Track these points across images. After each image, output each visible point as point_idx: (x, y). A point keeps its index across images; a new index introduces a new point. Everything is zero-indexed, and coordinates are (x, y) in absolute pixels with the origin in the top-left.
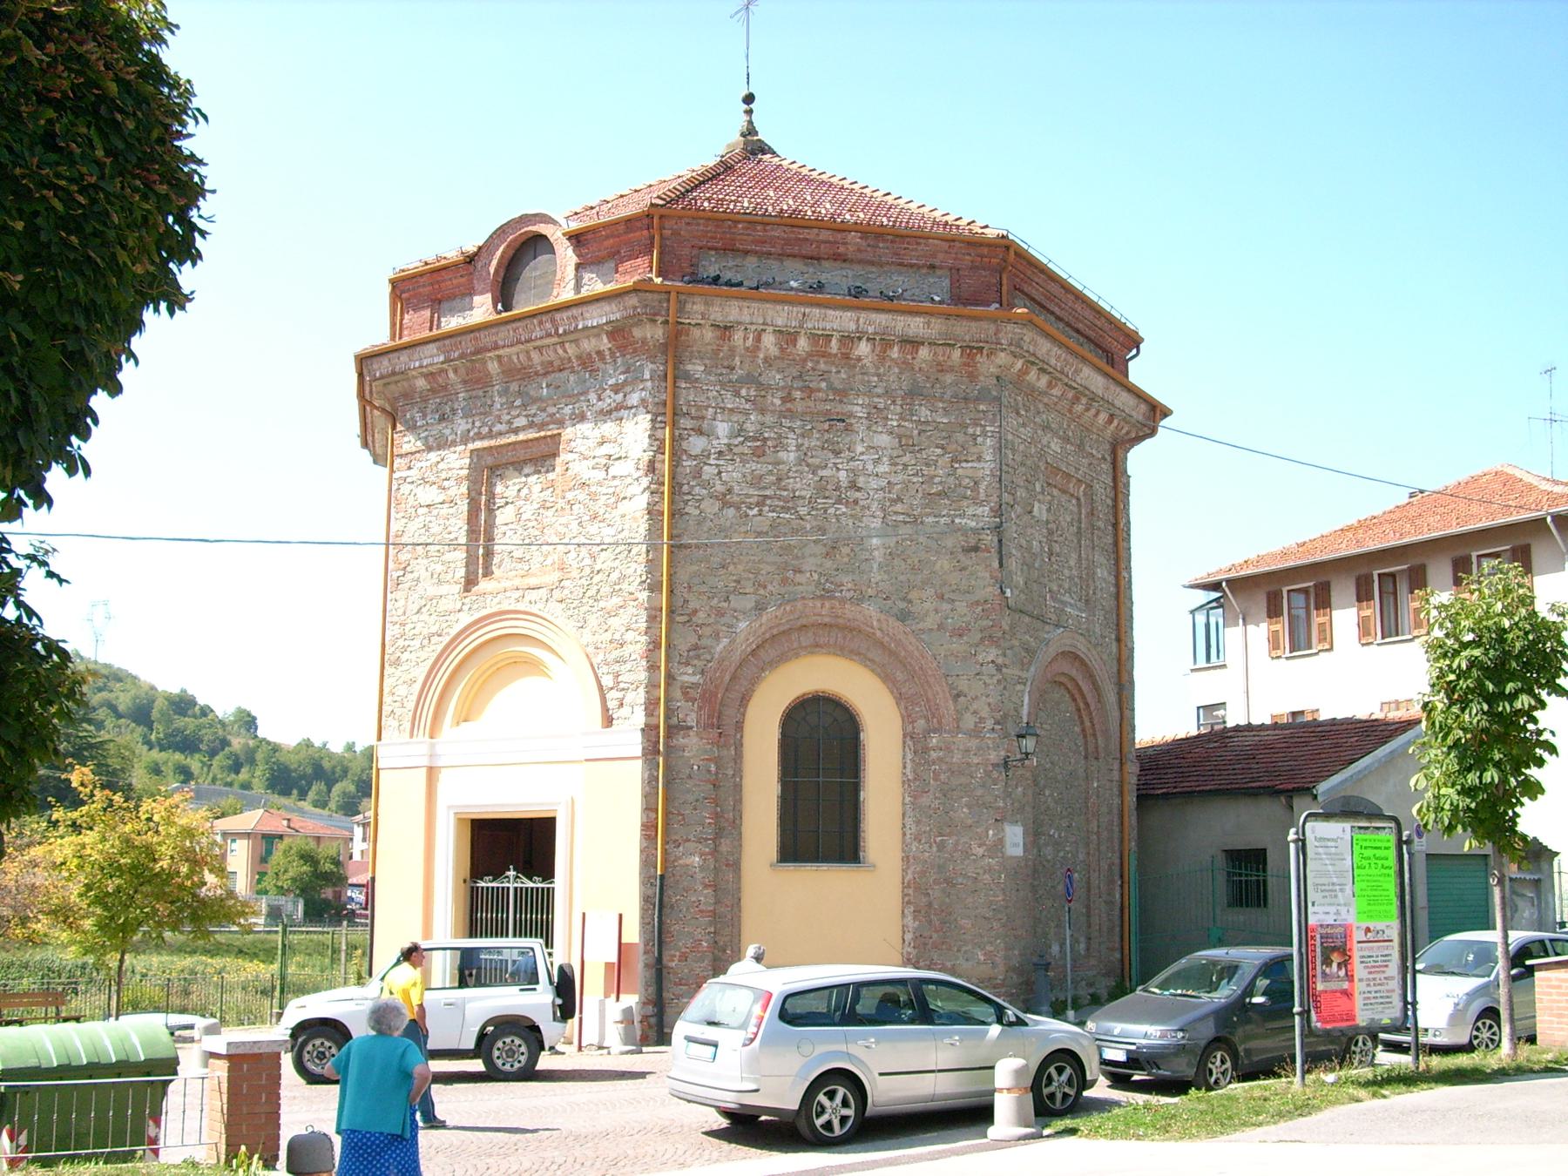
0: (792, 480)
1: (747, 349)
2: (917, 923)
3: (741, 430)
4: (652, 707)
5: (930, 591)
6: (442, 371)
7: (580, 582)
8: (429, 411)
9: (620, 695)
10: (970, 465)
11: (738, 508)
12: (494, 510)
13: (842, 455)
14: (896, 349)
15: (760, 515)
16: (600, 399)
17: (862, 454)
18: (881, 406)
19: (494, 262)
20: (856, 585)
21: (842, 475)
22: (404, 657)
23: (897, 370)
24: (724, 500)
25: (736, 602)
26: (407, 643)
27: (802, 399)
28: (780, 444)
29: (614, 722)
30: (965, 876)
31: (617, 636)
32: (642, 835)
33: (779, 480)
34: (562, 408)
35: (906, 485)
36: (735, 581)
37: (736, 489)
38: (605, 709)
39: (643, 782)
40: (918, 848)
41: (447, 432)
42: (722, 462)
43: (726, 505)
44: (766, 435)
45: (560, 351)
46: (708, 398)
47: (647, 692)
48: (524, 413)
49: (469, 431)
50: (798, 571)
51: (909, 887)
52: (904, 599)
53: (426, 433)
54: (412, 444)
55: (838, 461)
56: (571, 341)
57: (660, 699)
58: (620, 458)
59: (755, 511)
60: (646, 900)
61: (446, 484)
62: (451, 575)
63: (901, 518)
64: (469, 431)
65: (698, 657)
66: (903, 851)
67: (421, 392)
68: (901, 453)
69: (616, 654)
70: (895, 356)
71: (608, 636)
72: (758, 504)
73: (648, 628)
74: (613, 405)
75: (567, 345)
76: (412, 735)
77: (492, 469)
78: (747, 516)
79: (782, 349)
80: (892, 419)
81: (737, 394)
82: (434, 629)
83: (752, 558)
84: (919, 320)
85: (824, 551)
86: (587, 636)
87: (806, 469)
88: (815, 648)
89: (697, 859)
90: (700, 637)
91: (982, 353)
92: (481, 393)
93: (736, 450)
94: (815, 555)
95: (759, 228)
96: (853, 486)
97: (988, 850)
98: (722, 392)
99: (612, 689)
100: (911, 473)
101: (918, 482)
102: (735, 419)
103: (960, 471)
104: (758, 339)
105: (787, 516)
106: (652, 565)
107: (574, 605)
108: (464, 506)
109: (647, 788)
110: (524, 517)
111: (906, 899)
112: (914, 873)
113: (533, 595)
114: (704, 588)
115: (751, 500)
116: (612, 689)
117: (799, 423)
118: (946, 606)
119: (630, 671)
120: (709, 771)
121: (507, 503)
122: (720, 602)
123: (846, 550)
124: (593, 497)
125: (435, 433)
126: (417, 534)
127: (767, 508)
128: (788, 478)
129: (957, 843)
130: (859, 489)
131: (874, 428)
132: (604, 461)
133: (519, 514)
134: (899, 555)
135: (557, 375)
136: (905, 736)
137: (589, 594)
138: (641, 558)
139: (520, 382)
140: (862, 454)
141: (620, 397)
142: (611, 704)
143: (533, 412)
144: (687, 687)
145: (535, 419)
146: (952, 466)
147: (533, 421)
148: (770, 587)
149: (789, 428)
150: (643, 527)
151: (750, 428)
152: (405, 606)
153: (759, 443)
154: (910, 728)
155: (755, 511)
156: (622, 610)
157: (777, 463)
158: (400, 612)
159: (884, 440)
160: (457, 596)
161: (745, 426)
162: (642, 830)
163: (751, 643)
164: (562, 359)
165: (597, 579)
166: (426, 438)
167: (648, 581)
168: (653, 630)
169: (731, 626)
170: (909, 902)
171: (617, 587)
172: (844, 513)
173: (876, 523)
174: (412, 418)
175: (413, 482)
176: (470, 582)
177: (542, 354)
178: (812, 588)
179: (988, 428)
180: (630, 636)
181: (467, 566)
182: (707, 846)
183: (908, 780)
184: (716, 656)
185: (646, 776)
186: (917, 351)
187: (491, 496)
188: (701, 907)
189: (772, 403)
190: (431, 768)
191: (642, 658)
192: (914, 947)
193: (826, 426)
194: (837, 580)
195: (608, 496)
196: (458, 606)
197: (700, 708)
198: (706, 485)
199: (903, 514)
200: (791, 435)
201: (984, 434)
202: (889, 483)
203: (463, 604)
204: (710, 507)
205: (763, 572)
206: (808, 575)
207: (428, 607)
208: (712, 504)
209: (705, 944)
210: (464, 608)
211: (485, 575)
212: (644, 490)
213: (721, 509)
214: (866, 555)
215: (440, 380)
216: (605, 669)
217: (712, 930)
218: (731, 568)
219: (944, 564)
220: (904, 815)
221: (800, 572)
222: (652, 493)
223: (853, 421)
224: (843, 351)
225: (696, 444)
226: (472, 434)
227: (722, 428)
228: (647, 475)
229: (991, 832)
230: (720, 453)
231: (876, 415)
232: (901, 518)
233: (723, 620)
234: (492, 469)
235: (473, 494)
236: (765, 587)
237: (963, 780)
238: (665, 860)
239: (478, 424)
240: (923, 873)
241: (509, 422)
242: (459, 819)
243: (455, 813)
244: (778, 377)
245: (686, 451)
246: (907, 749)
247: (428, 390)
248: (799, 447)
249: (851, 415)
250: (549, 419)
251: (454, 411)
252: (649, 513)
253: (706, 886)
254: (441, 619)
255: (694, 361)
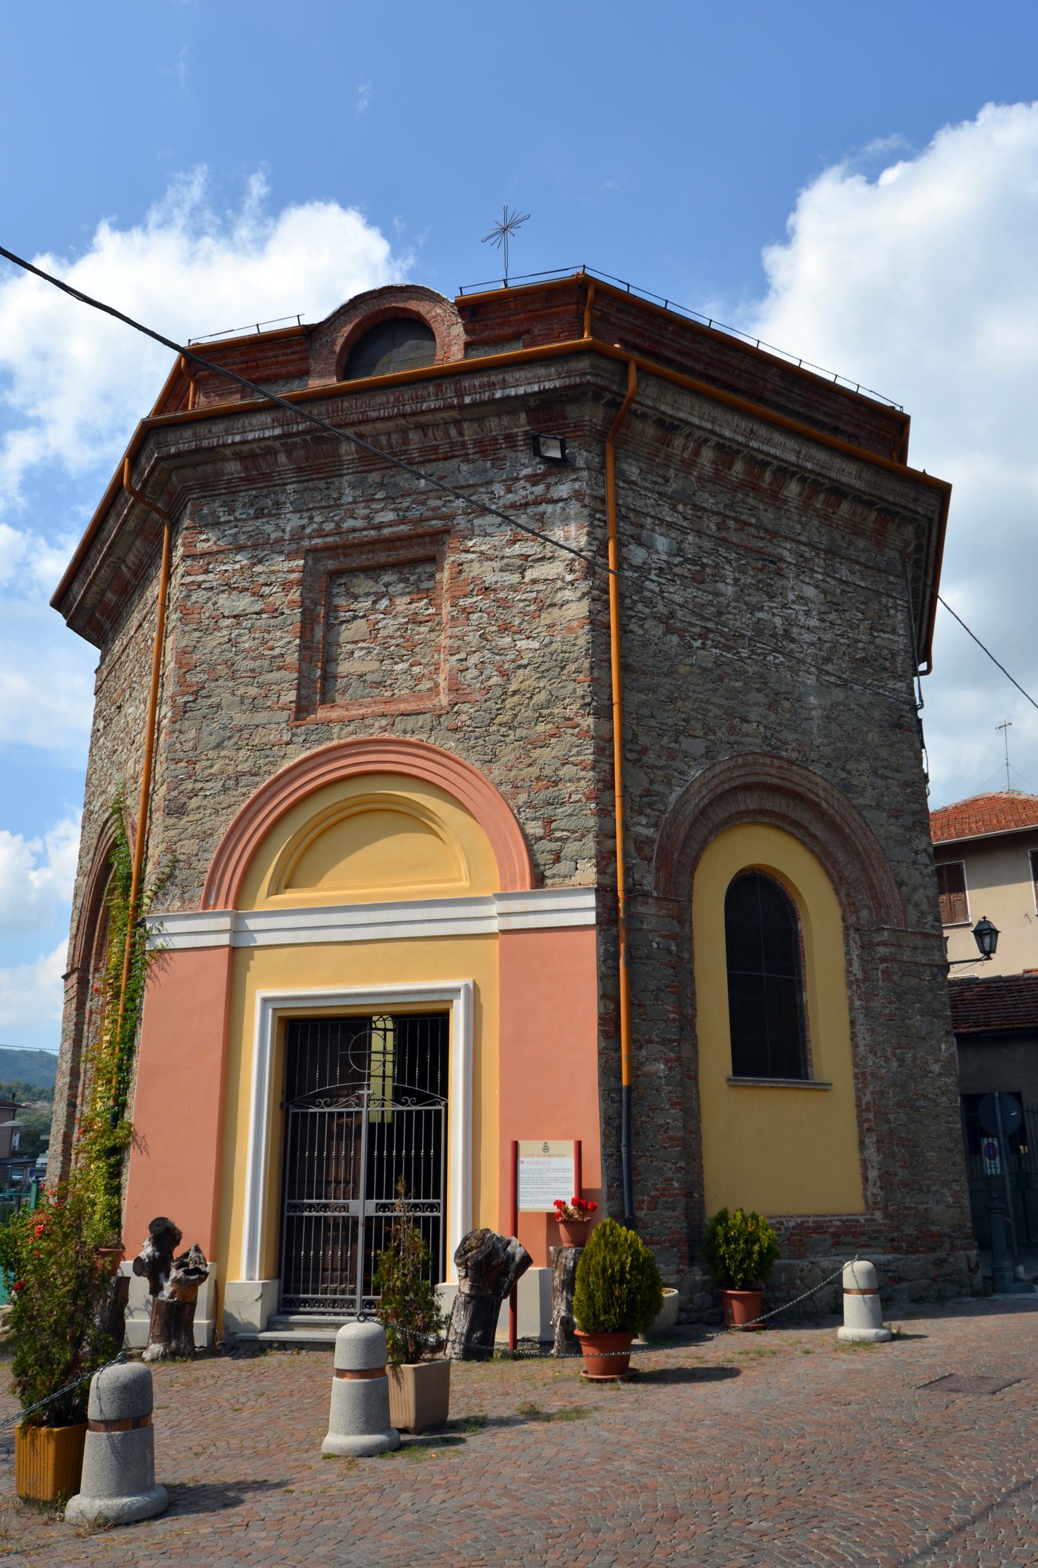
0: (731, 616)
1: (683, 461)
2: (881, 1156)
3: (679, 549)
4: (604, 863)
5: (865, 765)
6: (271, 452)
7: (485, 706)
8: (238, 505)
9: (555, 846)
10: (886, 636)
11: (682, 637)
12: (334, 625)
13: (776, 600)
14: (822, 497)
15: (703, 648)
16: (509, 491)
17: (793, 602)
18: (807, 555)
19: (340, 341)
20: (799, 745)
21: (778, 620)
22: (194, 803)
23: (817, 523)
24: (667, 620)
25: (686, 743)
26: (199, 785)
27: (736, 530)
28: (718, 577)
29: (549, 881)
30: (925, 1097)
31: (548, 772)
32: (599, 1031)
33: (720, 613)
34: (450, 501)
35: (835, 644)
36: (684, 720)
37: (679, 613)
38: (534, 865)
39: (598, 960)
40: (874, 1062)
41: (269, 528)
42: (663, 581)
43: (670, 631)
44: (705, 561)
45: (453, 432)
46: (646, 504)
47: (599, 843)
48: (393, 506)
49: (303, 527)
50: (745, 720)
51: (867, 1110)
52: (843, 769)
53: (236, 530)
54: (211, 543)
55: (772, 605)
56: (471, 420)
57: (615, 852)
58: (543, 559)
59: (698, 644)
60: (607, 1121)
61: (266, 590)
62: (274, 698)
63: (832, 679)
64: (303, 527)
65: (650, 805)
66: (855, 1065)
67: (229, 481)
68: (828, 610)
69: (544, 795)
70: (818, 506)
71: (534, 771)
72: (700, 636)
73: (595, 761)
74: (531, 498)
75: (465, 425)
76: (206, 906)
77: (334, 575)
78: (691, 647)
79: (717, 471)
80: (817, 572)
81: (674, 509)
82: (244, 767)
83: (700, 696)
84: (852, 468)
85: (766, 701)
86: (497, 772)
87: (745, 607)
88: (759, 817)
89: (662, 1066)
90: (652, 782)
91: (893, 521)
92: (322, 484)
93: (677, 570)
94: (757, 704)
95: (688, 336)
96: (787, 635)
97: (942, 1067)
98: (660, 502)
99: (541, 838)
100: (838, 632)
101: (844, 644)
102: (674, 535)
103: (878, 641)
104: (697, 453)
105: (729, 655)
106: (599, 685)
107: (476, 734)
108: (295, 616)
109: (603, 968)
110: (383, 633)
111: (866, 1125)
112: (873, 1093)
113: (410, 723)
114: (652, 723)
115: (694, 630)
116: (541, 838)
117: (734, 555)
118: (881, 783)
119: (570, 815)
120: (669, 952)
121: (355, 618)
122: (670, 743)
123: (786, 704)
124: (504, 604)
125: (250, 529)
126: (217, 651)
127: (709, 643)
128: (729, 613)
129: (915, 1058)
130: (793, 640)
131: (802, 577)
132: (519, 562)
133: (374, 630)
134: (834, 719)
135: (441, 464)
136: (846, 928)
137: (500, 719)
138: (581, 677)
139: (382, 472)
140: (793, 602)
141: (539, 489)
142: (541, 858)
143: (405, 505)
144: (642, 842)
145: (407, 514)
146: (871, 634)
147: (405, 517)
148: (719, 734)
149: (725, 558)
150: (583, 640)
151: (690, 552)
152: (197, 739)
153: (698, 568)
154: (852, 919)
155: (698, 644)
156: (553, 740)
157: (717, 594)
158: (187, 746)
159: (810, 592)
160: (283, 725)
161: (683, 546)
162: (599, 1024)
163: (704, 797)
164: (452, 444)
165: (510, 702)
166: (235, 535)
167: (594, 703)
168: (601, 764)
169: (682, 773)
170: (869, 1130)
171: (544, 712)
172: (782, 663)
173: (811, 681)
174: (213, 513)
175: (212, 588)
176: (302, 709)
177: (425, 435)
178: (758, 741)
179: (899, 602)
180: (567, 771)
181: (298, 689)
182: (672, 1050)
183: (857, 980)
184: (671, 806)
185: (602, 951)
186: (839, 506)
187: (332, 610)
188: (671, 1133)
189: (708, 526)
190: (234, 948)
191: (588, 799)
192: (881, 1188)
193: (759, 564)
194: (782, 735)
195: (526, 603)
196: (286, 737)
197: (658, 869)
198: (649, 603)
199: (835, 675)
200: (727, 567)
201: (895, 606)
202: (819, 639)
203: (293, 735)
204: (655, 630)
205: (711, 714)
206: (755, 725)
207: (234, 740)
208: (656, 626)
209: (676, 1185)
210: (296, 739)
211: (323, 702)
212: (584, 595)
213: (665, 634)
214: (804, 714)
215: (264, 465)
216: (529, 813)
217: (683, 1164)
218: (679, 703)
219: (873, 736)
220: (852, 1023)
221: (747, 721)
222: (593, 600)
223: (784, 566)
224: (774, 488)
225: (638, 555)
226: (308, 531)
227: (662, 543)
228: (585, 579)
229: (943, 1046)
230: (661, 569)
231: (803, 567)
232: (832, 679)
233: (675, 764)
234: (334, 575)
235: (307, 603)
236: (714, 733)
237: (914, 982)
238: (632, 1069)
239: (318, 519)
240: (882, 1094)
241: (368, 517)
242: (280, 1018)
243: (275, 1010)
244: (711, 501)
245: (627, 559)
246: (852, 943)
247: (242, 479)
248: (736, 580)
249: (782, 559)
250: (430, 513)
251: (278, 505)
252: (591, 623)
253: (673, 1105)
254: (258, 753)
255: (629, 461)
